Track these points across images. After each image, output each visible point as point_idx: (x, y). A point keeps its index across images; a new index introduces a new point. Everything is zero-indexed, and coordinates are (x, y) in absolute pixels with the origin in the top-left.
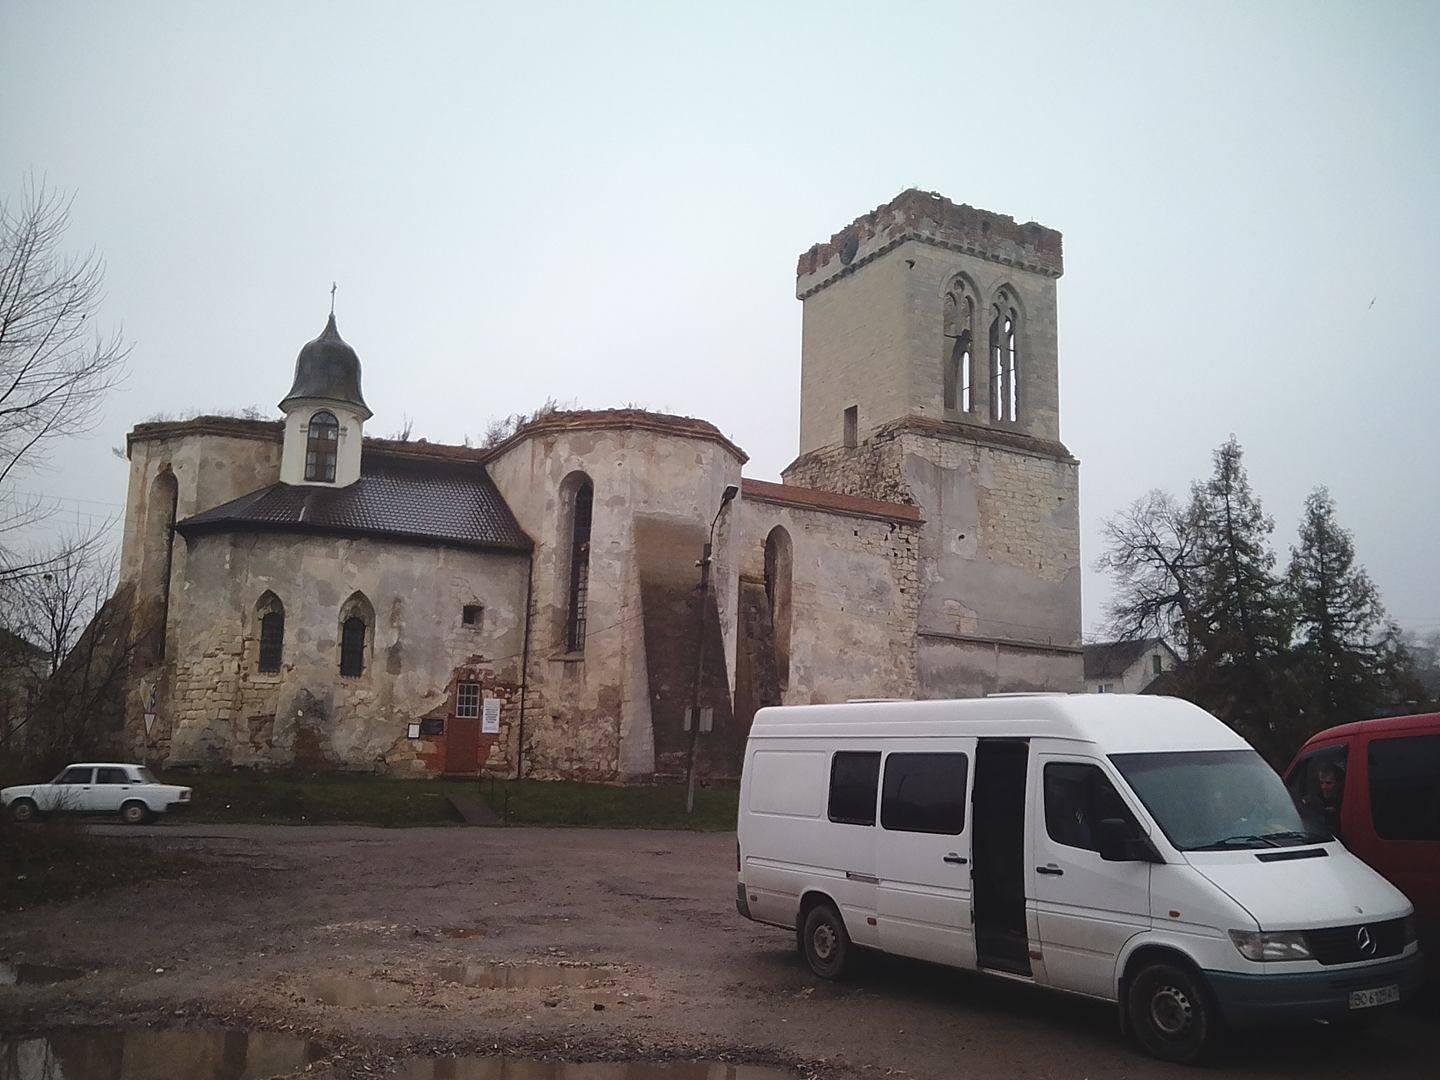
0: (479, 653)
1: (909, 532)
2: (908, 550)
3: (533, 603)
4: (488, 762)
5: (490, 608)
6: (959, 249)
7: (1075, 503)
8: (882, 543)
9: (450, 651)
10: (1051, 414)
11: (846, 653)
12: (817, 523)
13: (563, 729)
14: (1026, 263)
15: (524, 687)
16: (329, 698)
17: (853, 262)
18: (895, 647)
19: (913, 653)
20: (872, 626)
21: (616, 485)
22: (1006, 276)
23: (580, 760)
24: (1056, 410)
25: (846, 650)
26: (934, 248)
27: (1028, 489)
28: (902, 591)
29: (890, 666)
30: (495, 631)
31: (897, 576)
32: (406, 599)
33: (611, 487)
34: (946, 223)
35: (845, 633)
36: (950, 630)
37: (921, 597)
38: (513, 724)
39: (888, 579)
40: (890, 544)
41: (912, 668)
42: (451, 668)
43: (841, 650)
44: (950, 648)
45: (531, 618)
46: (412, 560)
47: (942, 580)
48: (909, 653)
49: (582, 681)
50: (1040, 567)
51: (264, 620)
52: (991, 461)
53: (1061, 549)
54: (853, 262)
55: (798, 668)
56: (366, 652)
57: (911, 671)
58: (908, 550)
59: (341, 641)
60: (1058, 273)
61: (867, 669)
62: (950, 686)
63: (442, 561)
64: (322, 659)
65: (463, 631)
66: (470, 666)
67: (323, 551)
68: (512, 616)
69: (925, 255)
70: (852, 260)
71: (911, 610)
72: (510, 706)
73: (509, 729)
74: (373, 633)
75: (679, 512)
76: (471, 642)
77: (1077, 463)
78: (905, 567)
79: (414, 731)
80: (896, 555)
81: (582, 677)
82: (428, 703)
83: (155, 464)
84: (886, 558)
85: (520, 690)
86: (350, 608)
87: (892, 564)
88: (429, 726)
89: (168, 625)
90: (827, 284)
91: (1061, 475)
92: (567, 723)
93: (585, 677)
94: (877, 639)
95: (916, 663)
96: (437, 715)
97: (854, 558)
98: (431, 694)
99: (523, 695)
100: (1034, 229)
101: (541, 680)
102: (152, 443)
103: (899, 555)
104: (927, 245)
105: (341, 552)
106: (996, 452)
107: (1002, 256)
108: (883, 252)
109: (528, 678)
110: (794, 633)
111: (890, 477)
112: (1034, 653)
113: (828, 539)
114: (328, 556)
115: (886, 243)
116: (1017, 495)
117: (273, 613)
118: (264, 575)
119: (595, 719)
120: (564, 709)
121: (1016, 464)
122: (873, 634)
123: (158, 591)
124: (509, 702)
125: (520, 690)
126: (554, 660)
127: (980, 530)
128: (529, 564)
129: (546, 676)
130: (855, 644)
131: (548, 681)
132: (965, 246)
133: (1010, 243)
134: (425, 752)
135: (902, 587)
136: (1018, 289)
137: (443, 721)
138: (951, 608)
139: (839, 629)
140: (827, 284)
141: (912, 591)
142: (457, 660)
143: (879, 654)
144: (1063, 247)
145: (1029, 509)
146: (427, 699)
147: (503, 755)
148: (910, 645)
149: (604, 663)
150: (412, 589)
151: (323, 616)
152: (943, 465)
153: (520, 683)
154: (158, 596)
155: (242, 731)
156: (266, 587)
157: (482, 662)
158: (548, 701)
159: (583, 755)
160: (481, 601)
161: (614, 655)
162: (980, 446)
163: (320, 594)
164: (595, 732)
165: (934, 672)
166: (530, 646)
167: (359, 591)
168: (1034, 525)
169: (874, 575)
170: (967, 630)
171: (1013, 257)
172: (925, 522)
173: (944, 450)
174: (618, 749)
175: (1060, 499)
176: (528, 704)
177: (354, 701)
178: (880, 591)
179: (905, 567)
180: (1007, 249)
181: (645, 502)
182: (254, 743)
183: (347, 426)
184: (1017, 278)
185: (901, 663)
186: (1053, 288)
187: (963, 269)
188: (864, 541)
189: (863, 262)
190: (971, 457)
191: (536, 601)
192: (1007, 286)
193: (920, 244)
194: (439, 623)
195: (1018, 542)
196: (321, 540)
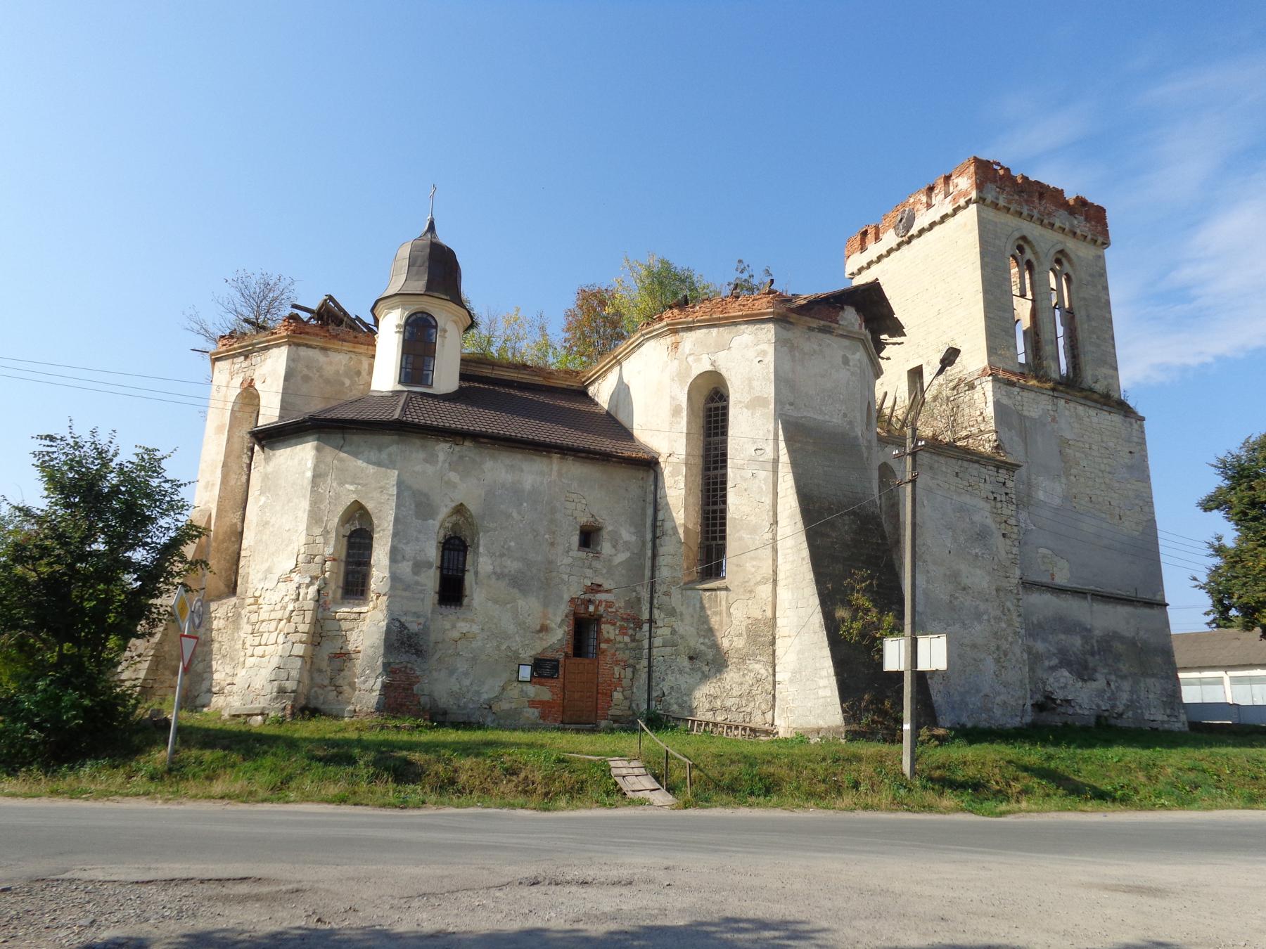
0: (598, 581)
1: (1007, 477)
2: (1007, 494)
3: (659, 524)
4: (610, 713)
5: (610, 528)
7: (1144, 458)
9: (565, 577)
10: (1111, 372)
11: (957, 598)
13: (703, 673)
14: (1078, 232)
15: (651, 621)
16: (426, 629)
17: (909, 234)
18: (1001, 594)
19: (1018, 600)
20: (978, 572)
21: (755, 383)
22: (1061, 243)
23: (728, 710)
24: (1116, 369)
25: (957, 595)
26: (997, 212)
27: (1102, 442)
28: (1004, 535)
29: (998, 613)
30: (615, 555)
31: (998, 520)
32: (515, 515)
33: (751, 387)
34: (1007, 189)
35: (954, 577)
36: (1045, 579)
37: (1021, 544)
38: (637, 666)
39: (989, 521)
40: (989, 487)
41: (1020, 616)
42: (567, 597)
43: (951, 595)
44: (1047, 597)
45: (658, 540)
46: (522, 471)
47: (1034, 528)
48: (1015, 601)
49: (725, 615)
50: (1120, 519)
51: (350, 537)
52: (1067, 413)
53: (1137, 502)
54: (909, 234)
56: (469, 578)
57: (1019, 619)
58: (1007, 494)
59: (439, 564)
60: (1106, 244)
61: (978, 616)
62: (1051, 636)
63: (554, 474)
64: (417, 583)
65: (582, 554)
66: (588, 596)
67: (421, 455)
68: (634, 538)
69: (990, 218)
70: (908, 231)
71: (1013, 556)
72: (634, 644)
73: (633, 672)
74: (476, 553)
75: (827, 418)
76: (590, 567)
77: (1142, 419)
79: (526, 673)
80: (995, 498)
81: (724, 608)
82: (541, 639)
83: (238, 380)
84: (986, 502)
85: (646, 627)
86: (450, 525)
88: (543, 668)
89: (243, 553)
90: (880, 258)
91: (1129, 429)
92: (707, 665)
93: (729, 608)
94: (985, 584)
95: (1021, 610)
96: (549, 655)
98: (544, 629)
99: (650, 631)
100: (1082, 202)
101: (672, 613)
102: (235, 360)
103: (998, 499)
104: (990, 209)
105: (441, 457)
106: (1072, 404)
107: (1057, 224)
108: (944, 218)
109: (656, 612)
111: (973, 426)
112: (1123, 604)
113: (933, 478)
114: (426, 461)
115: (949, 210)
116: (1094, 447)
117: (361, 529)
118: (352, 483)
119: (743, 659)
120: (703, 647)
121: (1089, 417)
122: (979, 579)
123: (235, 519)
124: (633, 640)
125: (646, 627)
126: (686, 589)
127: (1064, 480)
128: (652, 478)
129: (679, 608)
130: (964, 589)
131: (681, 614)
132: (1025, 213)
133: (1063, 213)
134: (538, 699)
135: (1004, 532)
136: (1072, 256)
137: (557, 661)
138: (1044, 556)
139: (948, 573)
140: (880, 258)
141: (1014, 536)
142: (573, 588)
143: (987, 600)
144: (1108, 221)
145: (1105, 461)
146: (541, 635)
147: (627, 703)
148: (1016, 592)
149: (751, 592)
150: (521, 504)
151: (420, 532)
152: (1026, 413)
153: (646, 616)
154: (236, 524)
155: (320, 671)
156: (353, 497)
157: (600, 591)
158: (682, 637)
159: (728, 703)
160: (601, 520)
161: (764, 581)
162: (1057, 397)
163: (416, 506)
164: (744, 675)
165: (1035, 622)
166: (657, 573)
167: (461, 504)
168: (1110, 476)
169: (977, 518)
170: (1061, 579)
171: (1067, 227)
172: (1020, 466)
173: (1026, 400)
174: (774, 696)
175: (1131, 452)
176: (657, 642)
177: (456, 635)
178: (982, 535)
180: (1061, 219)
181: (791, 404)
182: (335, 686)
183: (447, 328)
184: (1071, 245)
185: (1009, 610)
186: (1101, 258)
187: (1025, 233)
189: (921, 232)
190: (1050, 408)
191: (663, 520)
192: (1061, 252)
193: (986, 208)
194: (552, 544)
195: (1098, 492)
196: (418, 442)
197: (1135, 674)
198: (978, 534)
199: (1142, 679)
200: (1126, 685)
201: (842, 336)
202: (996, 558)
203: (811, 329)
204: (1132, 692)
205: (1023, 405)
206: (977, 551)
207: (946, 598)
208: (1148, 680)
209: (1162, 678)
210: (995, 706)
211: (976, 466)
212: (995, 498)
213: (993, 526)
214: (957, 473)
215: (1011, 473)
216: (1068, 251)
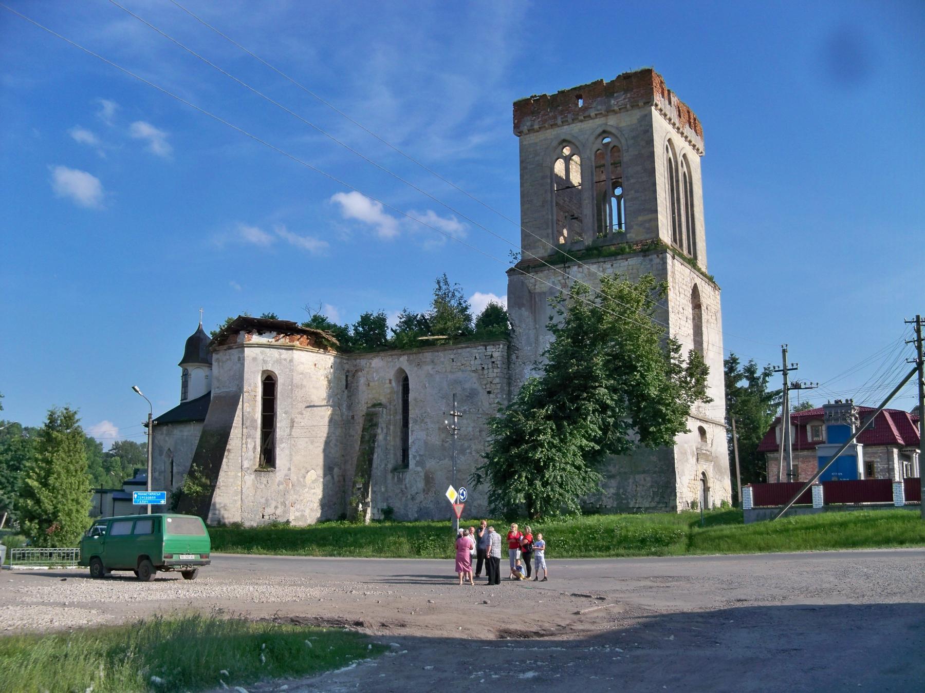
6: (553, 126)
8: (472, 362)
12: (425, 360)
31: (485, 382)
40: (478, 362)
43: (443, 441)
55: (414, 457)
58: (493, 362)
75: (231, 389)
78: (491, 375)
87: (479, 375)
97: (451, 377)
104: (531, 135)
105: (165, 432)
110: (412, 434)
135: (488, 390)
143: (471, 439)
178: (471, 396)
179: (491, 375)
181: (218, 388)
187: (563, 137)
188: (459, 364)
197: (625, 473)
198: (468, 396)
199: (632, 476)
200: (613, 483)
201: (236, 348)
202: (481, 409)
203: (225, 350)
204: (618, 488)
205: (535, 285)
206: (465, 408)
207: (438, 443)
208: (637, 477)
209: (655, 472)
210: (473, 507)
211: (468, 349)
212: (483, 368)
213: (480, 389)
214: (453, 359)
215: (497, 346)
216: (609, 129)
